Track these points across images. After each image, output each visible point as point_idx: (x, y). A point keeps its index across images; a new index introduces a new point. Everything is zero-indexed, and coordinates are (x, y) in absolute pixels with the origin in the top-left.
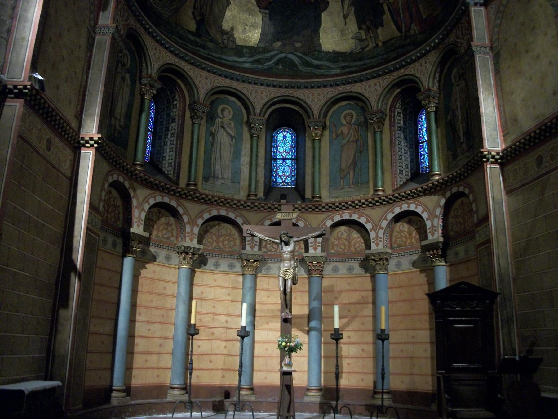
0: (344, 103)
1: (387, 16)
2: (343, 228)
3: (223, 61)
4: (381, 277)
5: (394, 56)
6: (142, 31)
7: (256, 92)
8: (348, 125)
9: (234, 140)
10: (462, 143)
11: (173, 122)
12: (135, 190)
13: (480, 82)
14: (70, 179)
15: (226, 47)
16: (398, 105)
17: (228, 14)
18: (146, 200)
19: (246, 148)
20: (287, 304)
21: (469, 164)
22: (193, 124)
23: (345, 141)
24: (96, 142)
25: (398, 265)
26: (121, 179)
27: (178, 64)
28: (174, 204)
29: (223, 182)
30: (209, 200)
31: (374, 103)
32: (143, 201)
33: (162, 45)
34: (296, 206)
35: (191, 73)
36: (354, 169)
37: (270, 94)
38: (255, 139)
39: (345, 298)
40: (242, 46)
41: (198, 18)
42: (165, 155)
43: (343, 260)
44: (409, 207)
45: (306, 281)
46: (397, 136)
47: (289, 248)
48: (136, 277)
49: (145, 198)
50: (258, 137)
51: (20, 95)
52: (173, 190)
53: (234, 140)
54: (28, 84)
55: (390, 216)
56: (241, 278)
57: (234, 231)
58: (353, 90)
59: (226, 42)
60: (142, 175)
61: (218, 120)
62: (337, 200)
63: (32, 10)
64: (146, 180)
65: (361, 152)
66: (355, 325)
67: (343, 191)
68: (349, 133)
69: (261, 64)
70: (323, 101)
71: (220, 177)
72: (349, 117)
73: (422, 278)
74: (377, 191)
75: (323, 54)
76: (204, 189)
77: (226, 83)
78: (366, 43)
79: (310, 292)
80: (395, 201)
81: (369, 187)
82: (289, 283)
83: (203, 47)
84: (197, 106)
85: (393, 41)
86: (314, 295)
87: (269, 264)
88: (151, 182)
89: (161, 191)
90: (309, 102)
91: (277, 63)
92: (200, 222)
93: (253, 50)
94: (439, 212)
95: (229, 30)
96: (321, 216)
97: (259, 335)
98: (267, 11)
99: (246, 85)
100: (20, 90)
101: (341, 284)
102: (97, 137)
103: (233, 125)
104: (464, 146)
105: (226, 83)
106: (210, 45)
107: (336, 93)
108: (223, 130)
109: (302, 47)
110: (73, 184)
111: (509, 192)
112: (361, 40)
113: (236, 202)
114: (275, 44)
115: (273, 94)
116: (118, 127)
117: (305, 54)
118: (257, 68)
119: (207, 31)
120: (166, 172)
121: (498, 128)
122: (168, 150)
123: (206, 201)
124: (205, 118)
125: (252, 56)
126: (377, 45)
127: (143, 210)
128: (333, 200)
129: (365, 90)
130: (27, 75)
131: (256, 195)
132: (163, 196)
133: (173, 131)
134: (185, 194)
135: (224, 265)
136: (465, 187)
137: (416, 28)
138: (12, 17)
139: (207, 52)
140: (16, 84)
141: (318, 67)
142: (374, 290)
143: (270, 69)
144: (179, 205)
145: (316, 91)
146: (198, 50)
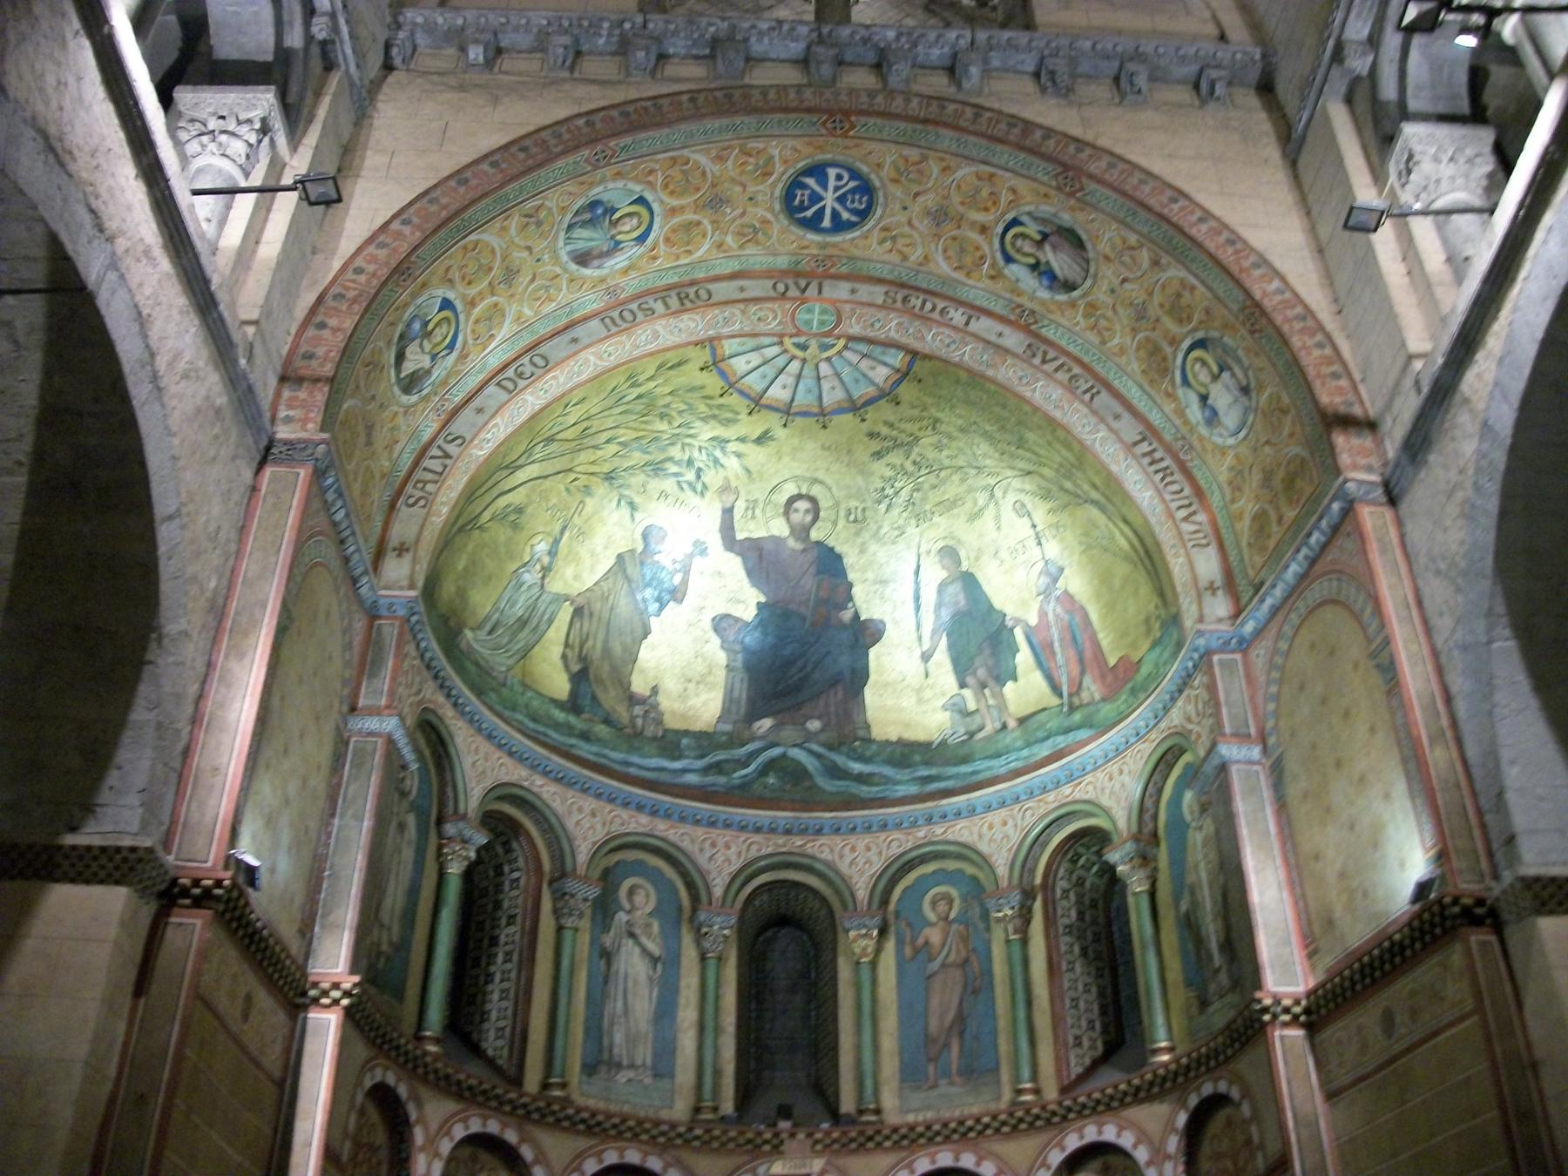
1: (1024, 657)
3: (632, 770)
5: (1046, 753)
6: (448, 713)
7: (713, 845)
8: (941, 923)
9: (659, 967)
10: (1218, 971)
11: (509, 924)
12: (420, 1105)
13: (1244, 831)
14: (280, 1084)
15: (639, 735)
16: (1061, 872)
18: (445, 1128)
19: (688, 987)
21: (1234, 1027)
22: (560, 929)
23: (935, 965)
24: (347, 994)
26: (391, 1079)
27: (526, 784)
28: (511, 1136)
29: (631, 1074)
30: (599, 1124)
32: (441, 1127)
33: (490, 737)
34: (819, 1136)
35: (557, 805)
36: (961, 1033)
37: (748, 849)
38: (712, 964)
40: (677, 732)
41: (576, 668)
42: (488, 1006)
44: (1100, 1133)
46: (1063, 948)
49: (446, 1121)
50: (719, 959)
51: (204, 899)
52: (510, 1101)
53: (659, 967)
54: (227, 877)
58: (950, 837)
59: (639, 722)
60: (439, 1065)
61: (622, 917)
62: (920, 1118)
63: (237, 705)
64: (447, 1077)
65: (975, 992)
67: (935, 1093)
68: (944, 945)
69: (727, 774)
70: (877, 866)
71: (625, 1062)
72: (943, 902)
74: (1019, 1092)
75: (874, 747)
76: (586, 1095)
77: (640, 823)
78: (977, 720)
80: (1064, 1118)
81: (998, 1082)
83: (585, 736)
84: (571, 885)
85: (1042, 716)
88: (459, 1083)
89: (480, 1105)
90: (844, 867)
91: (764, 771)
93: (705, 741)
94: (1173, 1144)
95: (648, 693)
96: (883, 1161)
99: (688, 828)
100: (207, 891)
102: (349, 982)
103: (656, 927)
104: (1224, 978)
106: (602, 730)
107: (910, 845)
108: (631, 942)
109: (823, 730)
110: (286, 1098)
111: (1331, 1095)
113: (665, 1128)
114: (757, 724)
115: (754, 847)
116: (385, 947)
117: (830, 747)
118: (714, 785)
119: (594, 698)
120: (490, 1052)
121: (1295, 939)
122: (496, 996)
123: (589, 1128)
124: (588, 913)
125: (702, 756)
126: (1004, 727)
127: (437, 1155)
128: (911, 1118)
129: (980, 836)
130: (222, 855)
131: (715, 1109)
132: (485, 1118)
133: (508, 948)
134: (538, 1109)
136: (1231, 1083)
137: (1093, 688)
138: (195, 720)
139: (595, 749)
140: (200, 875)
141: (861, 778)
143: (745, 786)
144: (523, 1140)
146: (572, 746)
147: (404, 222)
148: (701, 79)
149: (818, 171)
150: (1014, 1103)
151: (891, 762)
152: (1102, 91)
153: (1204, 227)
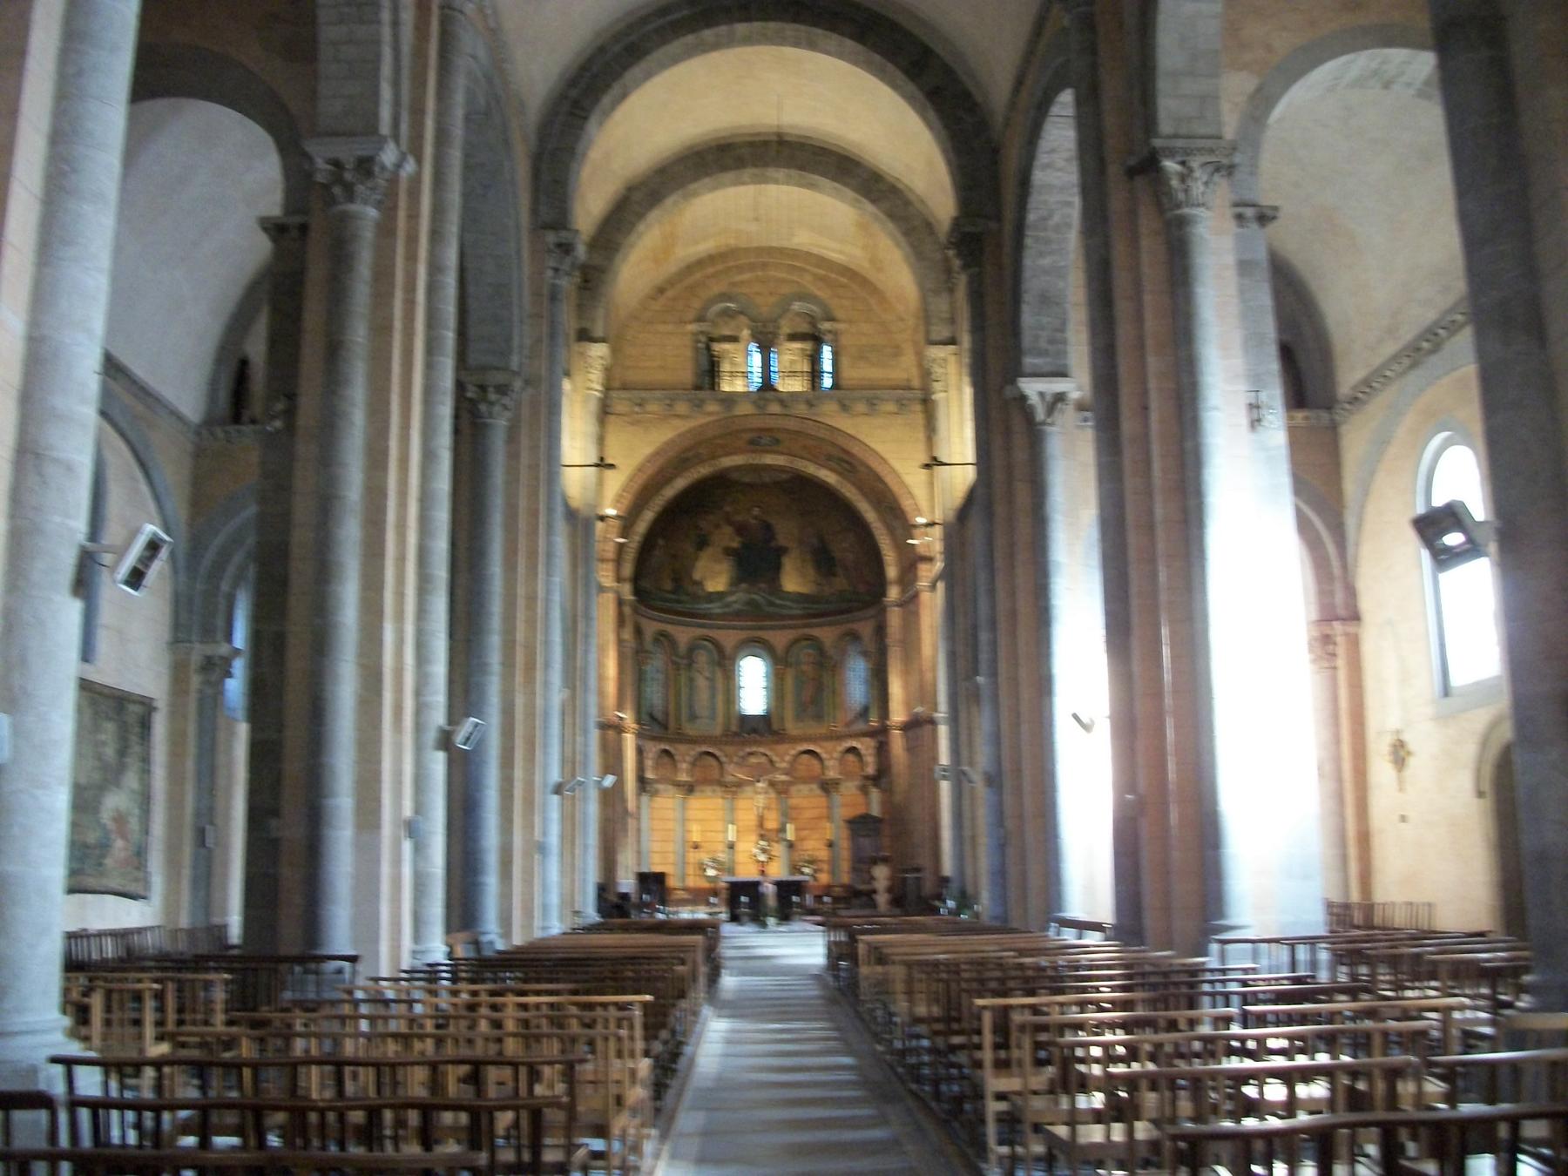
2: (806, 756)
20: (761, 824)
39: (808, 814)
73: (860, 799)
76: (690, 730)
83: (679, 602)
94: (871, 751)
97: (741, 847)
106: (684, 598)
135: (708, 790)
142: (830, 808)
148: (718, 413)
151: (792, 601)
152: (861, 407)
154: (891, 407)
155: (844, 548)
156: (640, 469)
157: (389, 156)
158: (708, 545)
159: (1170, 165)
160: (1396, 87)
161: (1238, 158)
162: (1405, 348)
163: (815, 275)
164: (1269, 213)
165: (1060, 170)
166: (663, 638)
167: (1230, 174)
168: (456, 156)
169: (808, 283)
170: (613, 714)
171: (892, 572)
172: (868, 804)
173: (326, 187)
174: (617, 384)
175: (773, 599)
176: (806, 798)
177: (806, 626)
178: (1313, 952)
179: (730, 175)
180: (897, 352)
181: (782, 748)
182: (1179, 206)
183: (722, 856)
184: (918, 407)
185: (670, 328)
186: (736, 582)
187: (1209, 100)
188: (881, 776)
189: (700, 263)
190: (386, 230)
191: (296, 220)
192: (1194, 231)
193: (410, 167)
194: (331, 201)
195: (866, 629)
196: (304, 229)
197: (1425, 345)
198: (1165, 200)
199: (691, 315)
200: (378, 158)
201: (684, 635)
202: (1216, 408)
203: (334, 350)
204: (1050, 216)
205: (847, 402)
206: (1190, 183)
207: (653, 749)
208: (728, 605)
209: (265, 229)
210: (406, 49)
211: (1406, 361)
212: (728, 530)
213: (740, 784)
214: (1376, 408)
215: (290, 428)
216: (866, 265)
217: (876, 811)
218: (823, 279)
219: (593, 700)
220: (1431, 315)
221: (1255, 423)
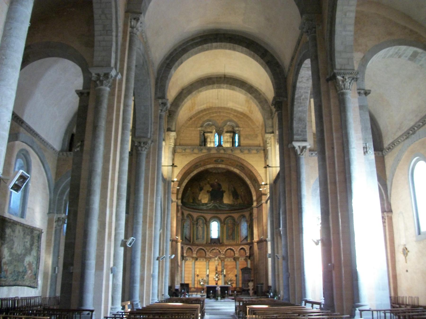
0: (229, 218)
1: (240, 197)
2: (229, 250)
4: (238, 262)
17: (200, 195)
20: (216, 270)
25: (241, 259)
31: (236, 219)
39: (230, 267)
43: (229, 258)
45: (221, 263)
47: (217, 258)
48: (185, 264)
55: (239, 248)
56: (205, 263)
57: (203, 252)
61: (199, 224)
66: (231, 273)
73: (245, 263)
74: (237, 242)
76: (197, 242)
77: (200, 214)
79: (222, 265)
82: (217, 265)
83: (194, 206)
86: (223, 266)
87: (212, 259)
91: (212, 207)
92: (196, 250)
93: (206, 204)
94: (248, 249)
96: (224, 247)
97: (210, 276)
98: (210, 194)
101: (229, 263)
105: (200, 214)
106: (196, 204)
112: (234, 202)
135: (202, 259)
141: (222, 207)
142: (236, 265)
145: (222, 215)
147: (180, 174)
149: (218, 160)
150: (236, 243)
152: (246, 151)
153: (254, 171)
154: (255, 151)
155: (241, 191)
156: (184, 168)
157: (113, 73)
158: (203, 190)
159: (339, 78)
160: (402, 57)
161: (358, 76)
162: (405, 133)
163: (233, 115)
164: (368, 92)
165: (304, 83)
166: (189, 216)
167: (356, 81)
168: (133, 74)
169: (231, 116)
170: (175, 237)
171: (254, 198)
172: (247, 264)
173: (95, 82)
174: (178, 144)
175: (221, 205)
176: (229, 262)
177: (230, 213)
178: (385, 313)
179: (211, 86)
180: (257, 136)
181: (223, 248)
182: (342, 90)
183: (205, 279)
184: (262, 152)
185: (193, 129)
186: (210, 200)
187: (350, 59)
188: (251, 256)
189: (202, 111)
190: (112, 94)
191: (86, 91)
192: (347, 96)
193: (119, 76)
194: (96, 85)
195: (247, 214)
196: (88, 93)
197: (411, 132)
198: (338, 88)
199: (199, 125)
200: (110, 74)
201: (195, 215)
202: (354, 148)
203: (95, 127)
204: (302, 96)
205: (242, 150)
206: (345, 82)
207: (186, 248)
208: (208, 207)
209: (78, 94)
210: (119, 43)
211: (405, 137)
212: (208, 186)
213: (211, 258)
214: (396, 150)
215: (82, 150)
216: (248, 112)
217: (249, 266)
218: (236, 116)
219: (169, 233)
220: (412, 124)
221: (365, 153)
